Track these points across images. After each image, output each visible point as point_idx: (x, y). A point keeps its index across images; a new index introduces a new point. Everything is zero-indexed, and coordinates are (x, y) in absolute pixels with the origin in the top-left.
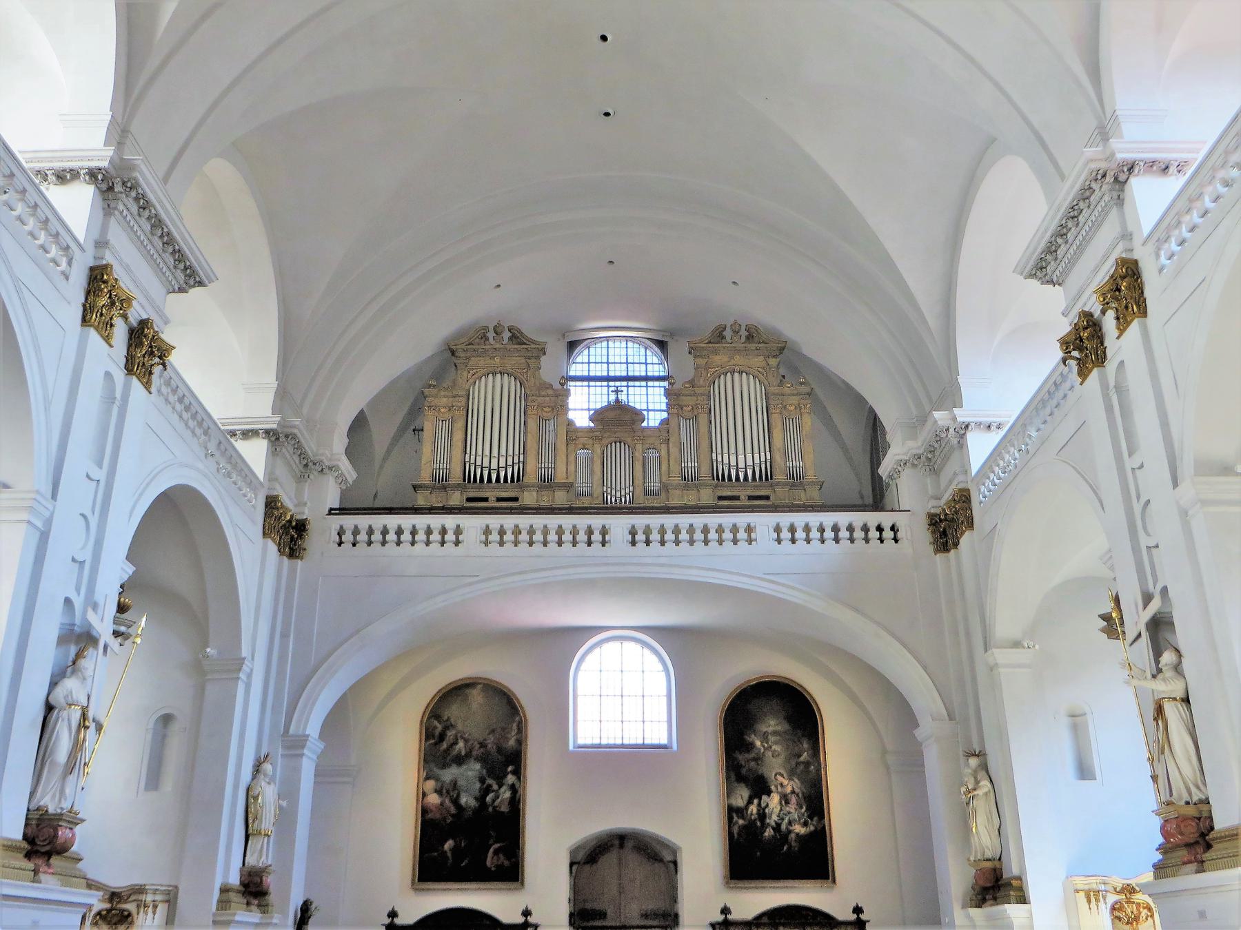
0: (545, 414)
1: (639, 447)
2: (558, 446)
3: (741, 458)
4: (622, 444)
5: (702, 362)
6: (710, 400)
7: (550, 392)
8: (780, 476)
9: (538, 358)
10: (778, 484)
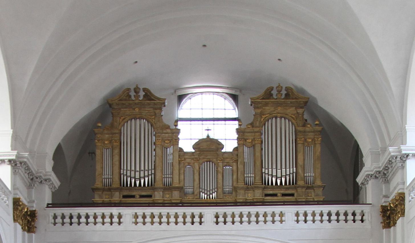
0: (166, 145)
1: (221, 164)
2: (174, 164)
3: (279, 171)
4: (211, 163)
5: (259, 111)
6: (261, 134)
7: (168, 131)
8: (300, 183)
9: (161, 109)
10: (299, 187)
